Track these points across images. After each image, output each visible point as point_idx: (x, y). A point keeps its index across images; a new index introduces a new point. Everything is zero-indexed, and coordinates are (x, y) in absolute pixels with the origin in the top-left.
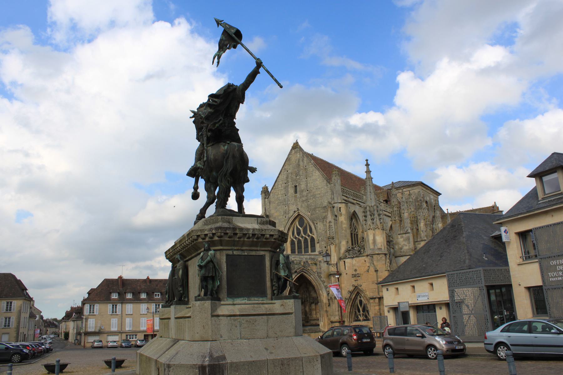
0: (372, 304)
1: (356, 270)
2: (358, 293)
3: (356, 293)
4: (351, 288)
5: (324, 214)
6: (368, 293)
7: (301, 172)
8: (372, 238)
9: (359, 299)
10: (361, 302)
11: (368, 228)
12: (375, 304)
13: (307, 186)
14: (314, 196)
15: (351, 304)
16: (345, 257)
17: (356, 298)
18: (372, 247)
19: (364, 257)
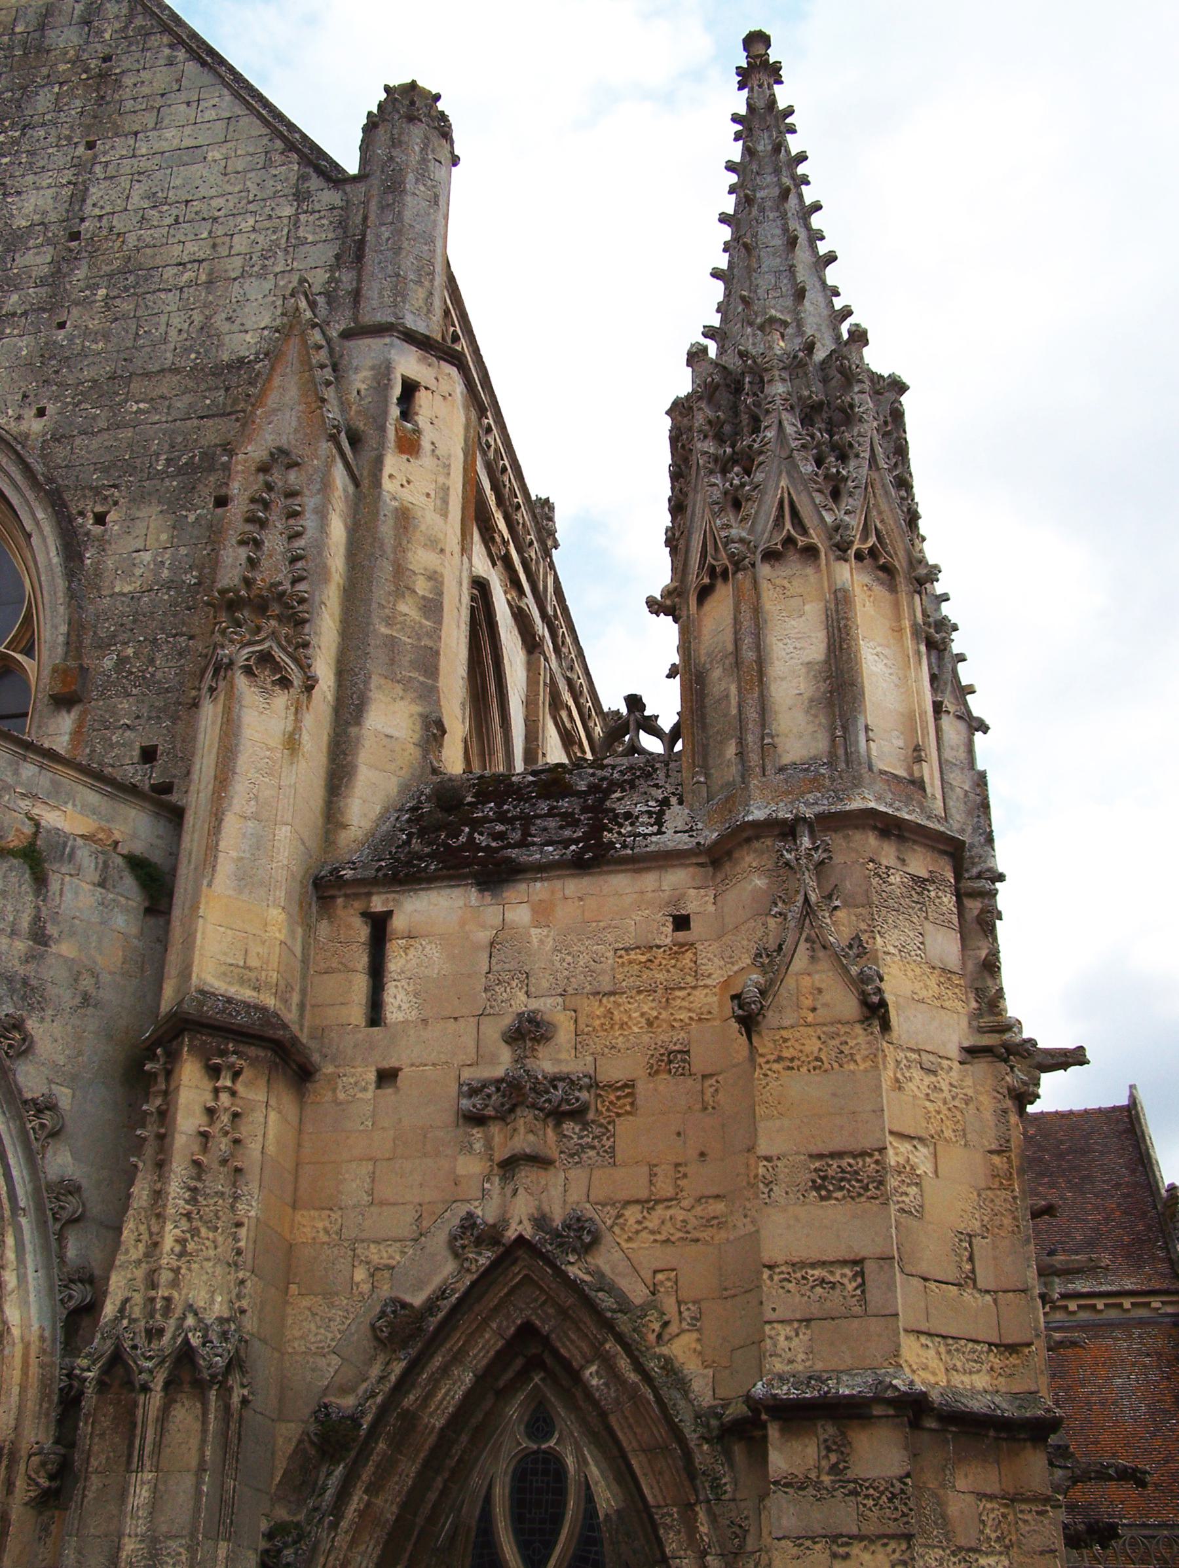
0: (785, 1514)
1: (528, 1032)
2: (528, 1352)
3: (485, 1347)
4: (433, 1274)
5: (212, 433)
6: (682, 1349)
7: (44, 100)
8: (815, 649)
9: (513, 1441)
10: (540, 1485)
11: (766, 535)
12: (843, 1515)
13: (79, 196)
14: (135, 275)
15: (388, 1507)
16: (405, 874)
17: (472, 1420)
18: (797, 734)
19: (676, 878)
